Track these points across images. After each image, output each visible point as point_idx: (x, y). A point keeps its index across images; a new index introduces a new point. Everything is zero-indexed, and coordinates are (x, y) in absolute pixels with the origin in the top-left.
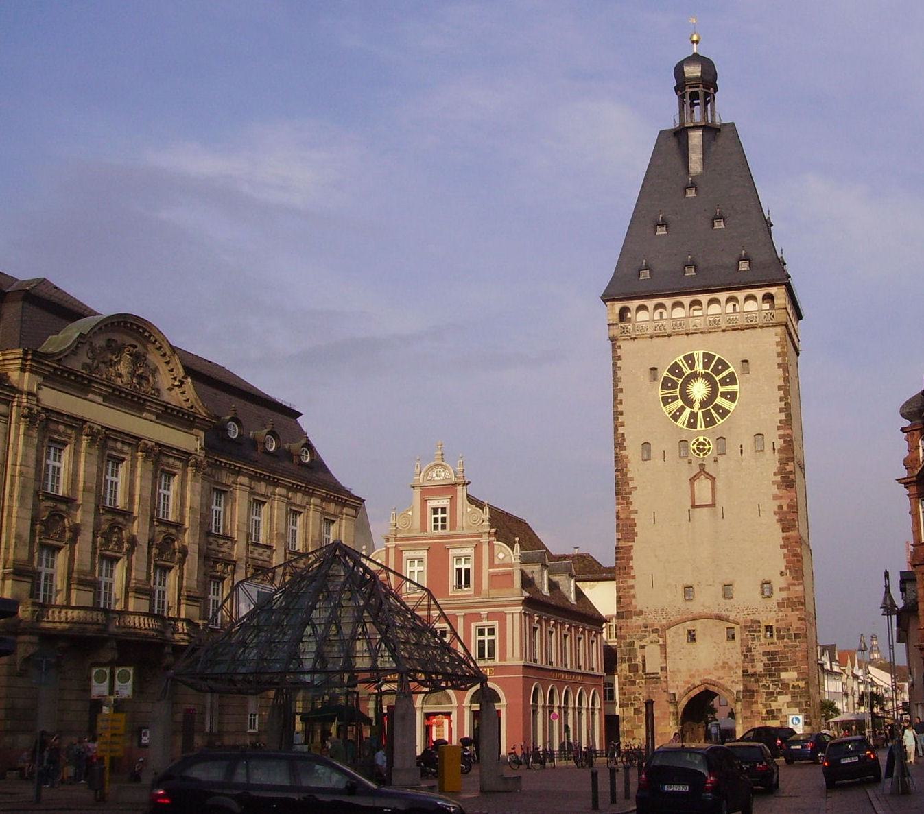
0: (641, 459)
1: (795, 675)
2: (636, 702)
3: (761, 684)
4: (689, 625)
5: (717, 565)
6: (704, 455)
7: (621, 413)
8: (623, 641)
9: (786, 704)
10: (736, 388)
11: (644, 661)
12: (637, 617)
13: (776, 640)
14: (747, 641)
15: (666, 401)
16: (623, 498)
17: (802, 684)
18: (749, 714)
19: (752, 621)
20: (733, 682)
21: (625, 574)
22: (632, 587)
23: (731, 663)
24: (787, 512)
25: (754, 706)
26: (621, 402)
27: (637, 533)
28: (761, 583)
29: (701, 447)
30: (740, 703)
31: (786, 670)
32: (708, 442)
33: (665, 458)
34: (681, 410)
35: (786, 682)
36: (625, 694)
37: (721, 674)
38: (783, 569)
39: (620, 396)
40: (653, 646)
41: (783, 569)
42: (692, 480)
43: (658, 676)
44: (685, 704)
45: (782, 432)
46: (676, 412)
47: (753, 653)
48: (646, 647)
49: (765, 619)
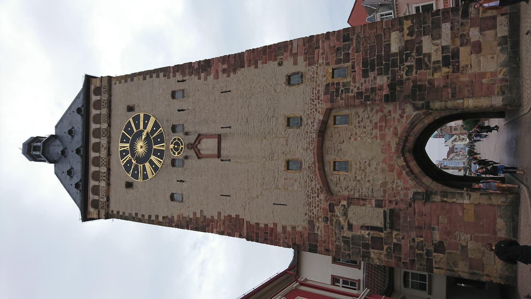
0: (181, 204)
1: (394, 35)
2: (425, 248)
3: (405, 77)
4: (329, 168)
5: (269, 133)
6: (182, 145)
7: (150, 216)
8: (342, 250)
9: (434, 42)
10: (142, 116)
11: (367, 228)
12: (316, 228)
13: (350, 63)
14: (348, 98)
15: (145, 177)
16: (208, 225)
17: (407, 24)
18: (449, 90)
19: (325, 94)
20: (401, 116)
21: (271, 235)
22: (284, 228)
23: (376, 118)
24: (228, 64)
25: (436, 83)
26: (143, 216)
27: (236, 215)
28: (287, 87)
29: (176, 146)
30: (431, 104)
31: (389, 46)
32: (175, 139)
33: (184, 181)
34: (152, 163)
35: (403, 44)
36: (413, 261)
37: (389, 133)
38: (276, 63)
39: (140, 216)
40: (350, 214)
41: (276, 63)
42: (199, 156)
43: (388, 212)
44: (420, 170)
45: (171, 74)
46: (153, 168)
47: (363, 90)
48: (351, 222)
49: (325, 79)
